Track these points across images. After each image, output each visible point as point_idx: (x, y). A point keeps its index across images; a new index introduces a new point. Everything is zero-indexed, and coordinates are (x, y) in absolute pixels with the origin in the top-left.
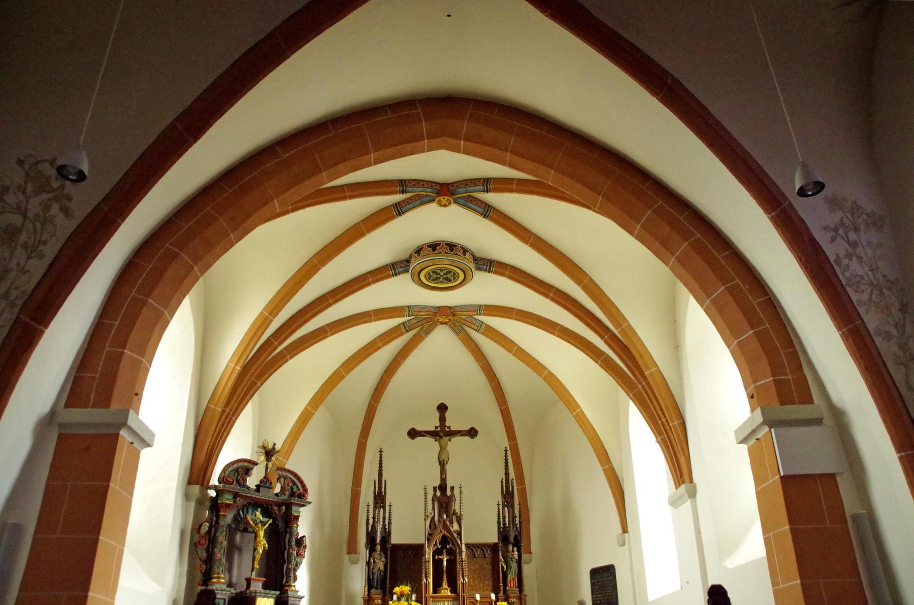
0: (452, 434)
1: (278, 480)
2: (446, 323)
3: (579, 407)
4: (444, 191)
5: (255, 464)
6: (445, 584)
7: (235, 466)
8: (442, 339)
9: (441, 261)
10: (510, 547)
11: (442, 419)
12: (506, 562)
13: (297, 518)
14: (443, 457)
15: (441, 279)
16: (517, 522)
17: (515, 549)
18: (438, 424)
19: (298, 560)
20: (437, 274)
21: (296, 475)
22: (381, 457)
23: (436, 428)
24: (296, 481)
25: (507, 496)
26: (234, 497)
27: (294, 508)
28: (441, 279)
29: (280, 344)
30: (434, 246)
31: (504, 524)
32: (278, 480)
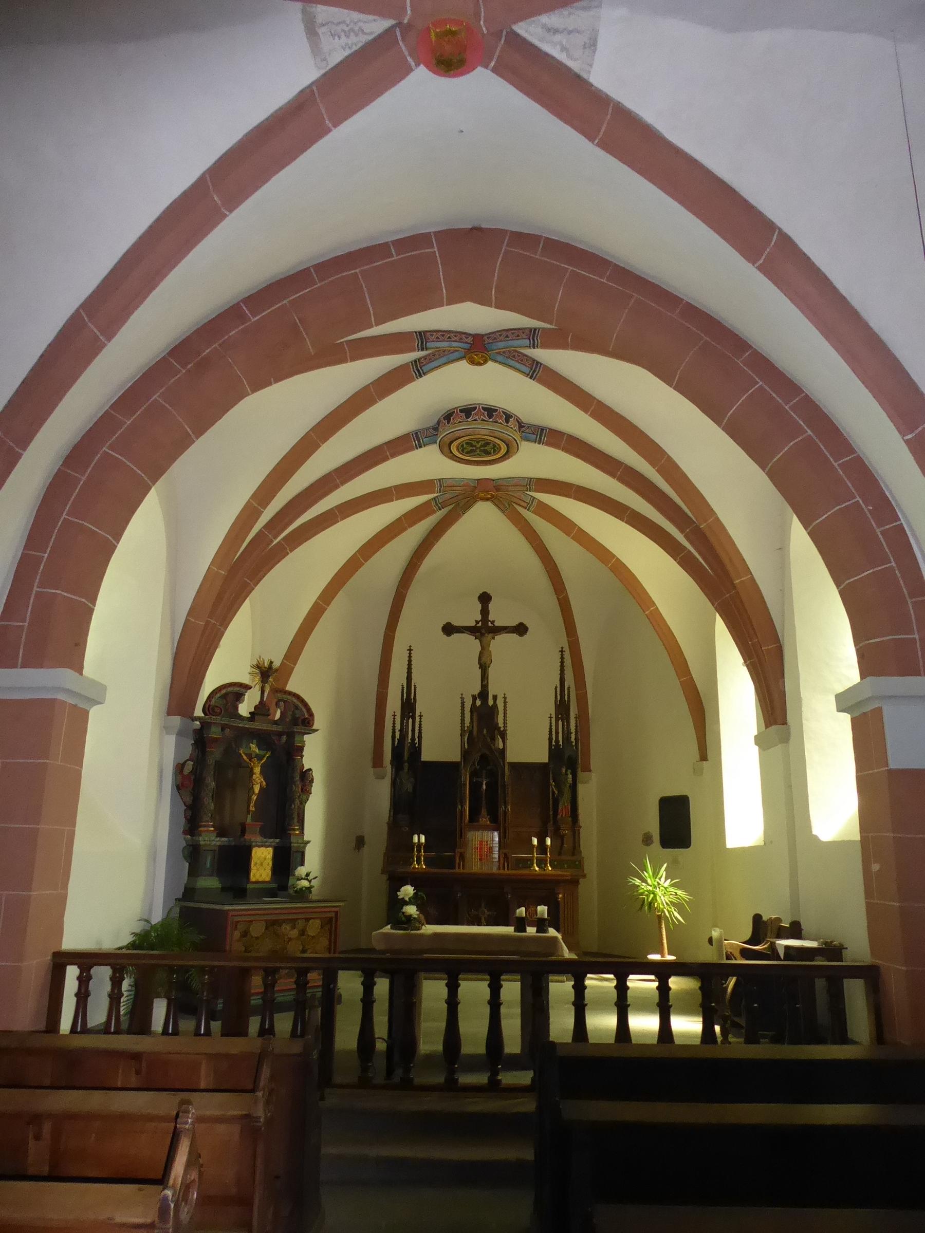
0: (497, 630)
1: (277, 705)
2: (487, 500)
3: (654, 604)
4: (477, 347)
5: (248, 687)
6: (484, 811)
7: (224, 691)
8: (483, 514)
9: (474, 432)
10: (564, 770)
11: (485, 612)
12: (558, 786)
13: (301, 749)
14: (483, 660)
15: (478, 452)
16: (573, 739)
17: (569, 771)
18: (479, 618)
19: (304, 797)
20: (472, 445)
21: (298, 697)
22: (410, 657)
23: (477, 622)
24: (300, 705)
25: (562, 708)
26: (223, 729)
27: (297, 738)
28: (478, 452)
29: (276, 538)
30: (467, 411)
31: (557, 741)
32: (277, 705)
